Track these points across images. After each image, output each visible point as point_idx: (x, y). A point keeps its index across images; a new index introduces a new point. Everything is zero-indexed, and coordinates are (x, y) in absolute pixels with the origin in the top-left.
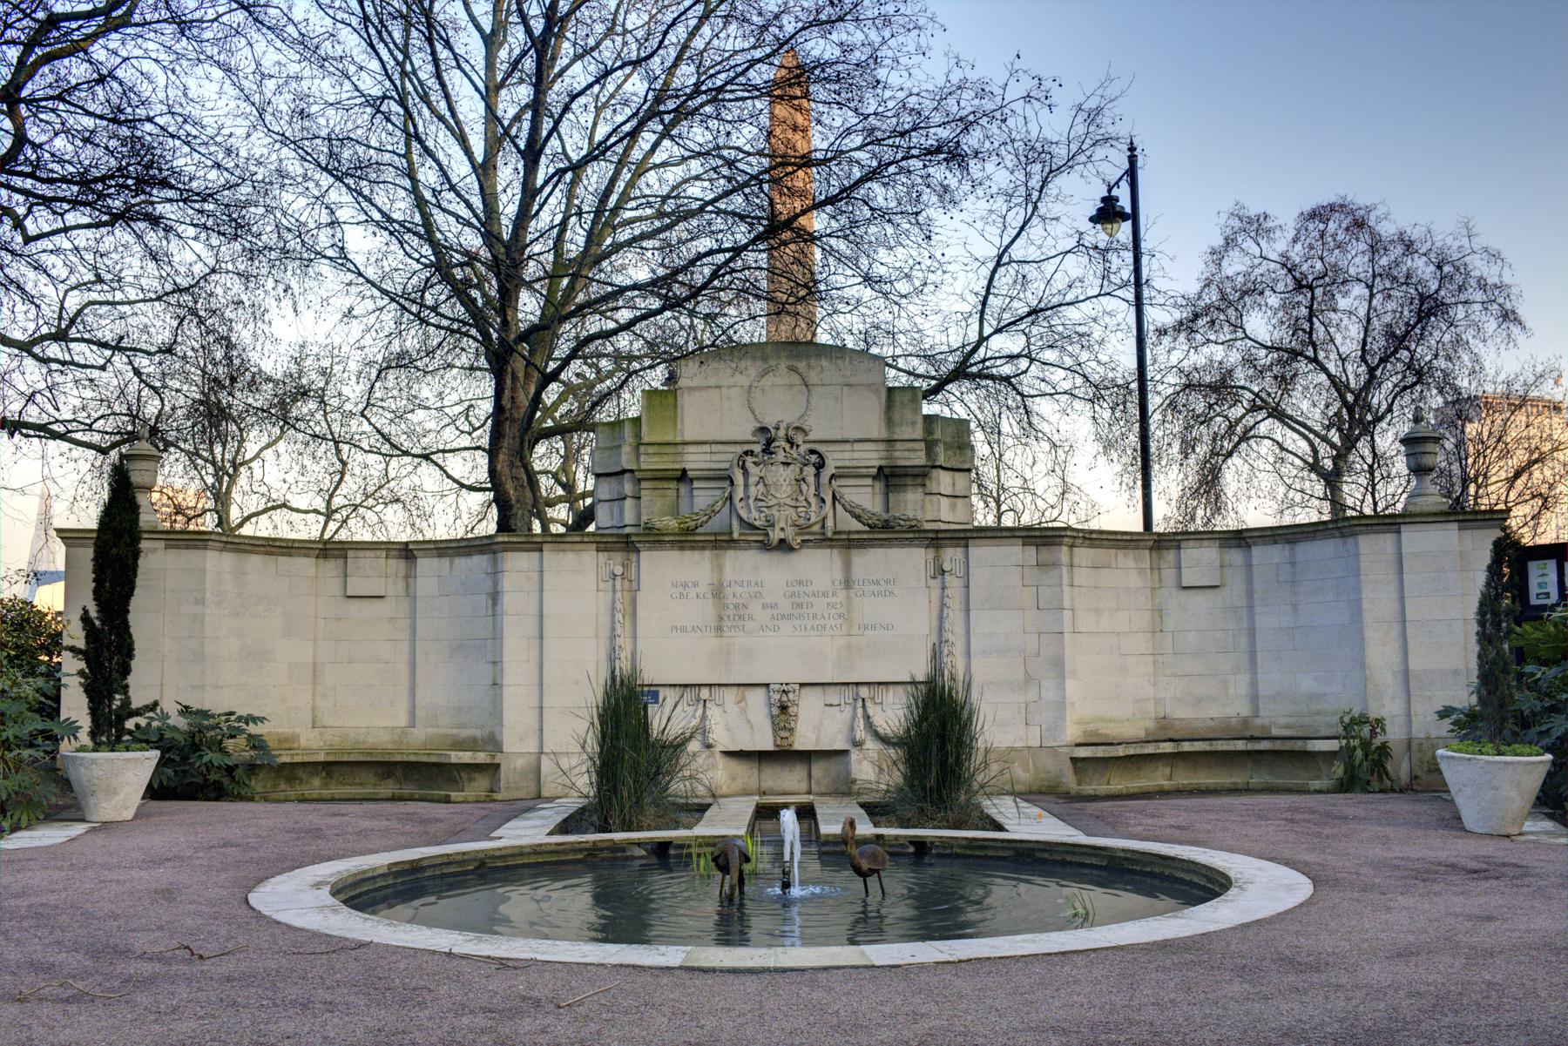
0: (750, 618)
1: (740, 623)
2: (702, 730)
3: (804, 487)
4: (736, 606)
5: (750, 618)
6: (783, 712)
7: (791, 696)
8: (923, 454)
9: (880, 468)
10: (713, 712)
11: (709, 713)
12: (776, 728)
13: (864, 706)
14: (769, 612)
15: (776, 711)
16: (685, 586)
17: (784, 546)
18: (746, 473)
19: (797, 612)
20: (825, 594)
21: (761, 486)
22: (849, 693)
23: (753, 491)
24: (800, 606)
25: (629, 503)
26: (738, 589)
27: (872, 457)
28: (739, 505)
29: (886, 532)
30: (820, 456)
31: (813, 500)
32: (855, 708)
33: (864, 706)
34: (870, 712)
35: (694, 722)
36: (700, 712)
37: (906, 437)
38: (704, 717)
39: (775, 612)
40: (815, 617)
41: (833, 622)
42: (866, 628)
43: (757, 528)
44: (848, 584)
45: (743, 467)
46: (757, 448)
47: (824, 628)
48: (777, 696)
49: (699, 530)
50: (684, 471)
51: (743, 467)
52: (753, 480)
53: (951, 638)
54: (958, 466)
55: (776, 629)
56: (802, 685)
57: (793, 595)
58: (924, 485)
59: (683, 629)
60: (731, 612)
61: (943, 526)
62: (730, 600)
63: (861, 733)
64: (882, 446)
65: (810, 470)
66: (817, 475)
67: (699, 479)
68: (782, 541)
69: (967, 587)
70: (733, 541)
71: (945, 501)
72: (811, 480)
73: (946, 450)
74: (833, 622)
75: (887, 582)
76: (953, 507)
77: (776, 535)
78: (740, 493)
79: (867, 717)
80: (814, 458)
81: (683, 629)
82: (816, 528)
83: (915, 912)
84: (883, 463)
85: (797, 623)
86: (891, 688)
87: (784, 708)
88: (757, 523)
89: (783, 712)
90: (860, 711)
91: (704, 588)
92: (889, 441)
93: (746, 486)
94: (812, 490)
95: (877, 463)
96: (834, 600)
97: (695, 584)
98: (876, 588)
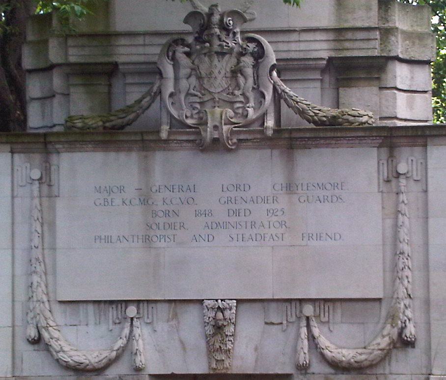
0: (182, 226)
1: (170, 232)
2: (126, 351)
3: (241, 80)
4: (167, 214)
5: (182, 226)
6: (218, 331)
7: (227, 313)
8: (377, 44)
9: (330, 59)
10: (142, 331)
11: (137, 332)
12: (211, 351)
13: (308, 326)
14: (202, 219)
15: (210, 330)
16: (110, 191)
17: (217, 146)
18: (176, 66)
19: (233, 219)
20: (265, 200)
21: (193, 80)
22: (293, 310)
23: (184, 84)
24: (237, 213)
25: (56, 101)
26: (167, 194)
27: (321, 49)
28: (168, 102)
29: (333, 131)
30: (259, 44)
31: (251, 95)
32: (299, 328)
33: (308, 326)
34: (316, 331)
35: (120, 343)
36: (127, 331)
37: (359, 24)
38: (130, 337)
39: (209, 219)
40: (253, 225)
41: (273, 231)
42: (310, 237)
43: (190, 127)
44: (290, 187)
45: (174, 59)
46: (190, 40)
47: (263, 238)
48: (212, 314)
49: (128, 129)
50: (116, 65)
51: (174, 59)
52: (184, 72)
53: (406, 248)
54: (418, 57)
55: (210, 239)
56: (239, 301)
57: (229, 201)
58: (378, 79)
59: (108, 240)
60: (161, 220)
61: (400, 124)
62: (160, 206)
63: (304, 356)
64: (331, 36)
65: (248, 61)
66: (256, 66)
67: (132, 74)
68: (215, 141)
69: (426, 191)
70: (160, 140)
71: (401, 96)
72: (249, 71)
73: (405, 39)
74: (273, 231)
75: (335, 186)
76: (410, 105)
77: (209, 133)
78: (169, 88)
79: (312, 338)
80: (252, 46)
81: (108, 240)
82: (256, 127)
83: (301, 364)
84: (333, 54)
85: (234, 232)
86: (338, 304)
87: (219, 328)
88: (189, 122)
89: (218, 331)
90: (304, 331)
91: (131, 193)
92: (339, 31)
93: (177, 79)
94: (251, 81)
95: (325, 55)
96: (276, 206)
97: (121, 189)
98: (321, 193)
